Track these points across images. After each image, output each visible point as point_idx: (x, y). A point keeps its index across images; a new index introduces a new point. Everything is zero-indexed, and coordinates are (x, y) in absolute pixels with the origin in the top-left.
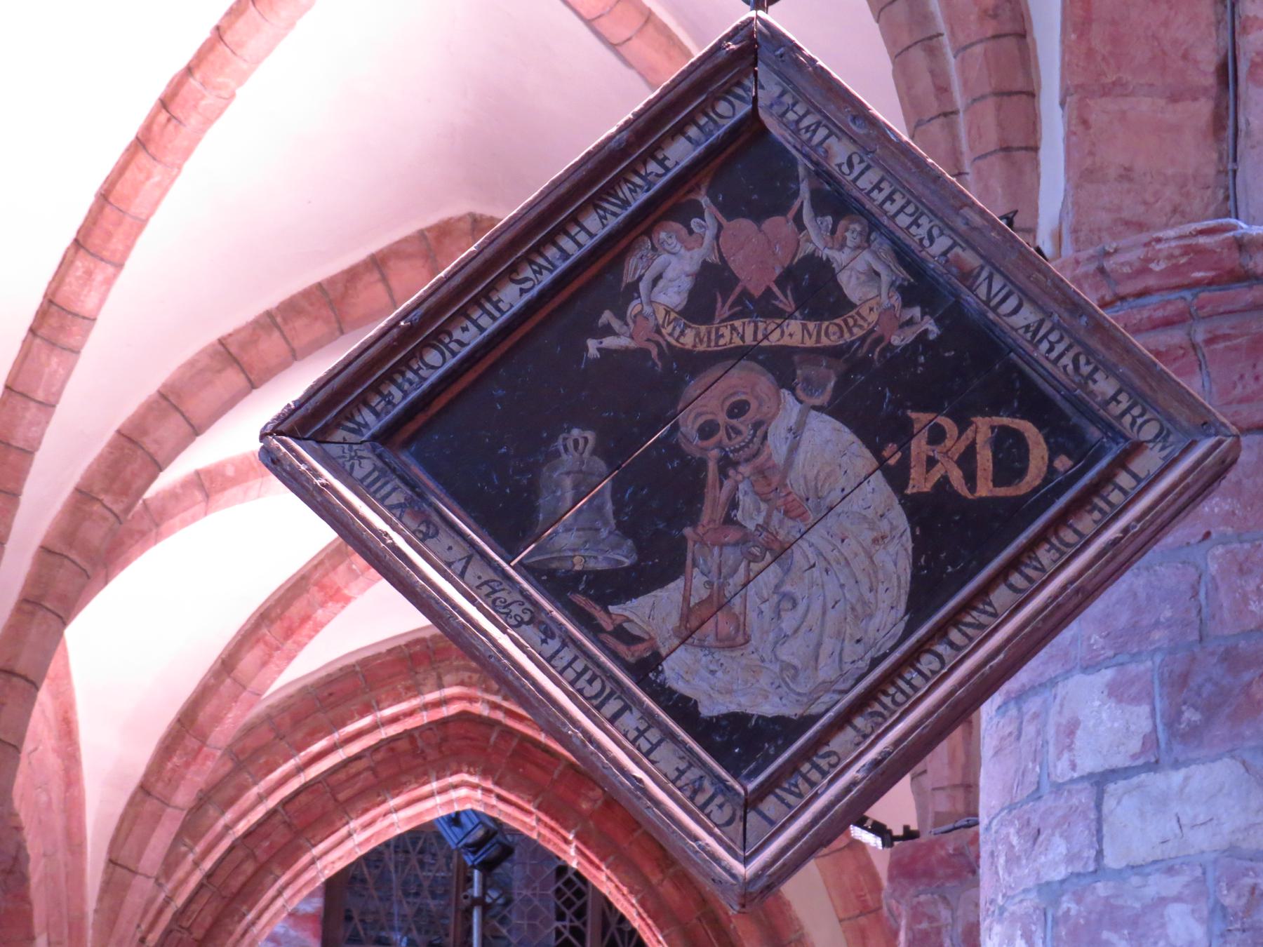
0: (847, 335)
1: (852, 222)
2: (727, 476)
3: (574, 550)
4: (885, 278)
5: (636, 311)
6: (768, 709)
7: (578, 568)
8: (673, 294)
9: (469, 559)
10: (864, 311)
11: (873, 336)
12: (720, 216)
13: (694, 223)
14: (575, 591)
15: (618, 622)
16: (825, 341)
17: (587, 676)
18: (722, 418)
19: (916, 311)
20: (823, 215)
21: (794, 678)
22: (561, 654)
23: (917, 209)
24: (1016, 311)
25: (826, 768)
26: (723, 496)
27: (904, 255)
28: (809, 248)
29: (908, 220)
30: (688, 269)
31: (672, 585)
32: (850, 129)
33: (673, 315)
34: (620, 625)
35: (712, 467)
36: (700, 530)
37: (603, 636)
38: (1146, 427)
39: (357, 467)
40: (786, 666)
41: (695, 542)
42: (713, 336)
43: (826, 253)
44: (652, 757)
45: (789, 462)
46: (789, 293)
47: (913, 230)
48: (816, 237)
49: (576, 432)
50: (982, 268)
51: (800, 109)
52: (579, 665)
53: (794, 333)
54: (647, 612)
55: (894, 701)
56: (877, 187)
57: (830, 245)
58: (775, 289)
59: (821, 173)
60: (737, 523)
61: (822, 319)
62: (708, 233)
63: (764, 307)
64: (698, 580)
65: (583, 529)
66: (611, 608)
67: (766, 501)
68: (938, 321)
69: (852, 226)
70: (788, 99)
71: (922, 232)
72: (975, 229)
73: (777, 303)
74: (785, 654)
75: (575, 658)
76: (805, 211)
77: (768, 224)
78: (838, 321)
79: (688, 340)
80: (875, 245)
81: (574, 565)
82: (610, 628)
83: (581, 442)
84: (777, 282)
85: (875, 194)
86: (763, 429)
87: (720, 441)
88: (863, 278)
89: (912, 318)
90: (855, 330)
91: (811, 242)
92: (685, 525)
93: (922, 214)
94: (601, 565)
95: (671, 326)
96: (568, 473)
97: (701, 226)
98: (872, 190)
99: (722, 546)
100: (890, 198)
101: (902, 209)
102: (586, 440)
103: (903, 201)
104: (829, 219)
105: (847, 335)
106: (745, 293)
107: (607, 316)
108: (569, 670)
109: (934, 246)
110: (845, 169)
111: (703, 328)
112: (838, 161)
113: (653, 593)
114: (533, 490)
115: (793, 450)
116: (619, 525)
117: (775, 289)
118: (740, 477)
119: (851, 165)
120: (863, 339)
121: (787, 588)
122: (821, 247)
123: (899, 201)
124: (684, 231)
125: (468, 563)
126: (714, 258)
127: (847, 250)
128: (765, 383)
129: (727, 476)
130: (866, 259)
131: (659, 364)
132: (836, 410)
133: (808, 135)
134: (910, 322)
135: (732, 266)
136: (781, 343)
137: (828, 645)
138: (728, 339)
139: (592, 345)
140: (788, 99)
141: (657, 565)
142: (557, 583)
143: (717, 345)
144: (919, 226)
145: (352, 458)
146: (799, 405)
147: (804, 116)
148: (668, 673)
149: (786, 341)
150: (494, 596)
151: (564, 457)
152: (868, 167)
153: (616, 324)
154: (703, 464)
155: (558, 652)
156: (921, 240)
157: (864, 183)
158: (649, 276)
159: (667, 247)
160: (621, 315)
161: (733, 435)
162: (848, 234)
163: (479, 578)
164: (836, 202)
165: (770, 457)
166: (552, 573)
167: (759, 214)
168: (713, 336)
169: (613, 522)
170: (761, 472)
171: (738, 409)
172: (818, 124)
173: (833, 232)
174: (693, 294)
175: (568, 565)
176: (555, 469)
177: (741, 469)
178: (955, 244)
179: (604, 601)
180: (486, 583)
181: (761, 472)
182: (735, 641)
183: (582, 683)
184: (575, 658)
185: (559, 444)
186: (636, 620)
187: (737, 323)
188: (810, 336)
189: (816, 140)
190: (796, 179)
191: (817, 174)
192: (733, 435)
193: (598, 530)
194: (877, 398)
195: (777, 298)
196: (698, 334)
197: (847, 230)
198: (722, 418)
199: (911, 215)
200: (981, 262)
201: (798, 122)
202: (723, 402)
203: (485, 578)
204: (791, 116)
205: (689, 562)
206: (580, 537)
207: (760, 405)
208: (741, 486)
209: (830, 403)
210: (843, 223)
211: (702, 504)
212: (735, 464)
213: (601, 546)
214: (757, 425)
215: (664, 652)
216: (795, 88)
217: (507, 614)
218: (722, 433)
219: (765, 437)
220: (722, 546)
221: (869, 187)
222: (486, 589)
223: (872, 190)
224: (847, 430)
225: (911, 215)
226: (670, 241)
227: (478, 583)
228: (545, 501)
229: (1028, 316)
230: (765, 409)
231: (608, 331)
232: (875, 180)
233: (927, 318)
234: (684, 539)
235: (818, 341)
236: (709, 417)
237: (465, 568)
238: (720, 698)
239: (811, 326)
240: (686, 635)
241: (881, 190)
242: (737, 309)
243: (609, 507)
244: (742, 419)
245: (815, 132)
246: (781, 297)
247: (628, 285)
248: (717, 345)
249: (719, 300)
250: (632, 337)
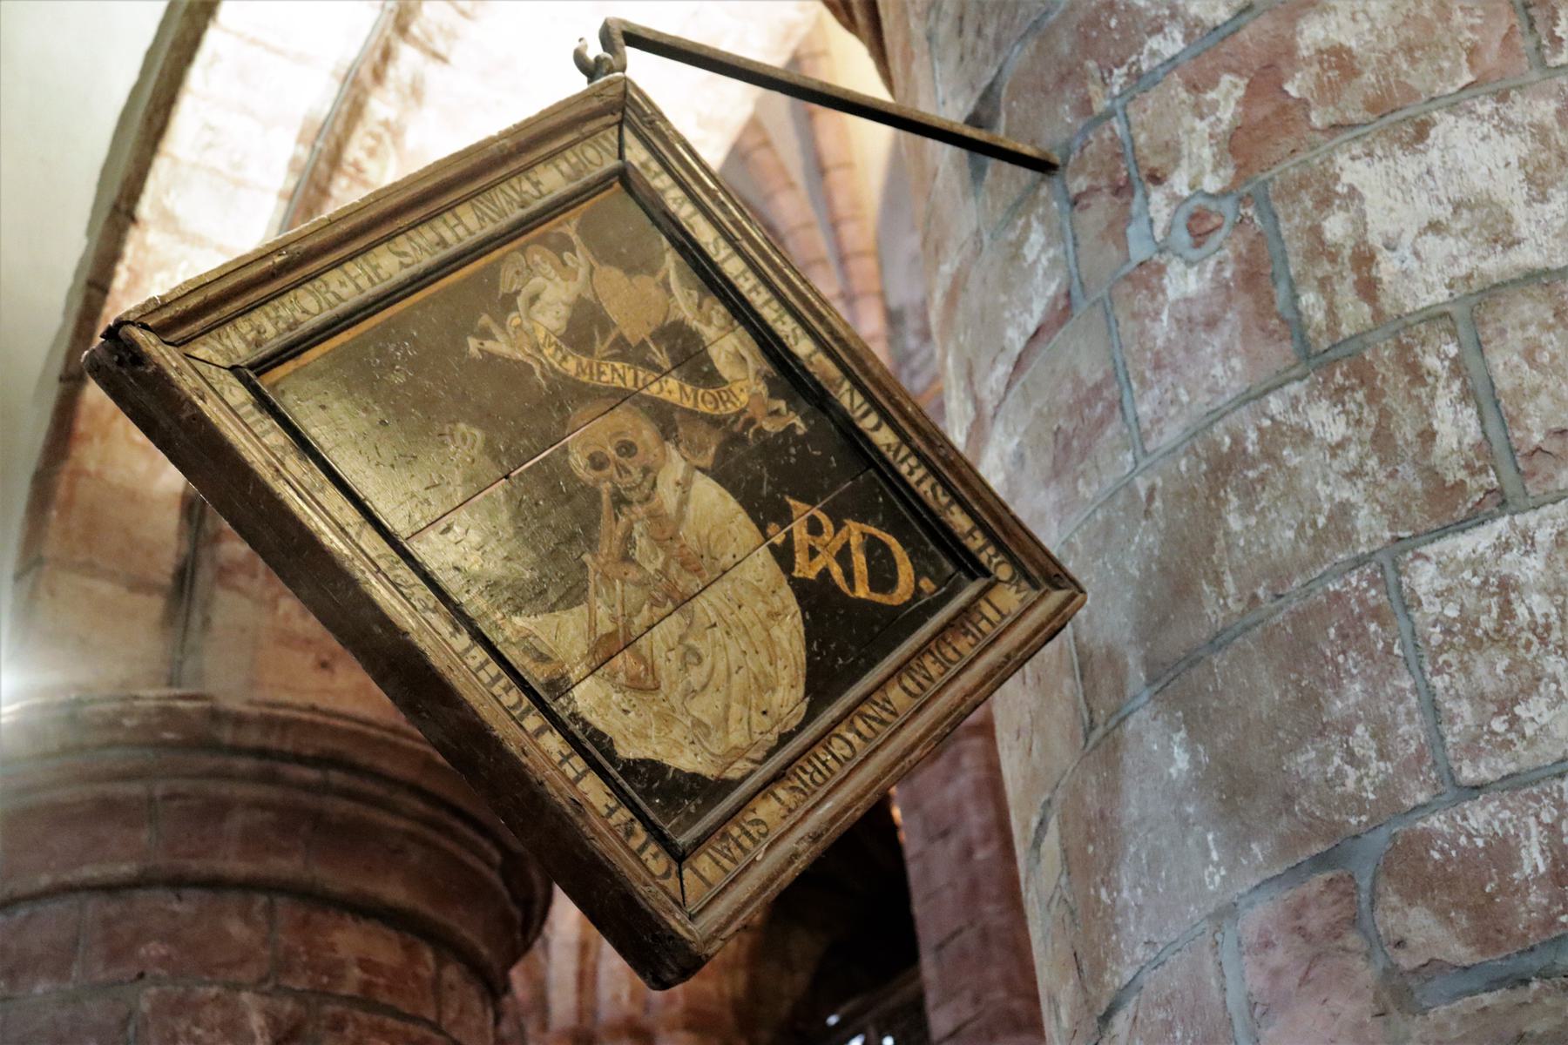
18: (611, 451)
30: (564, 297)
40: (698, 723)
45: (681, 515)
79: (571, 366)
84: (652, 337)
86: (651, 475)
107: (485, 319)
121: (691, 641)
124: (557, 262)
132: (722, 475)
137: (736, 709)
139: (473, 344)
153: (495, 330)
158: (526, 292)
170: (653, 516)
174: (572, 324)
198: (611, 451)
212: (629, 503)
215: (573, 677)
218: (611, 470)
219: (654, 485)
231: (486, 334)
238: (636, 742)
242: (615, 351)
247: (505, 296)
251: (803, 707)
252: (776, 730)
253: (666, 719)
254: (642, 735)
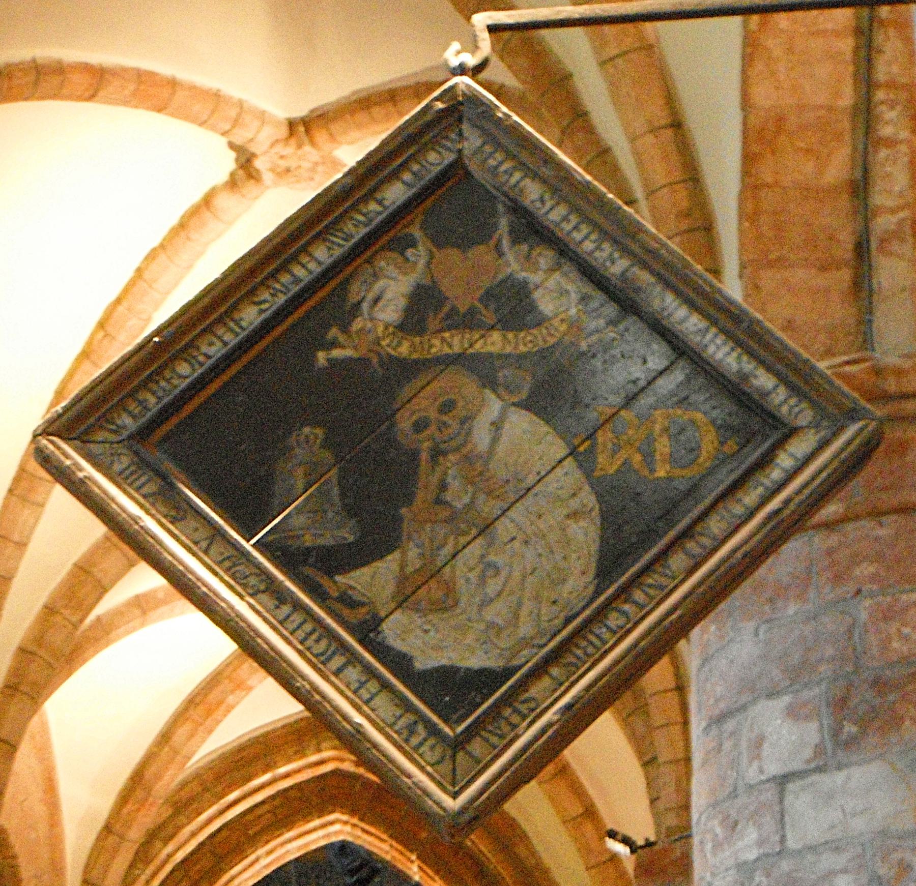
6: (475, 662)
7: (308, 544)
8: (390, 313)
18: (433, 414)
21: (498, 635)
25: (526, 712)
26: (435, 479)
33: (391, 329)
35: (424, 456)
36: (414, 508)
38: (800, 416)
40: (491, 625)
44: (372, 703)
48: (513, 263)
49: (307, 430)
55: (586, 653)
56: (565, 219)
64: (413, 553)
67: (472, 483)
74: (489, 614)
79: (404, 350)
82: (336, 594)
84: (481, 300)
94: (327, 540)
101: (586, 237)
107: (334, 332)
110: (538, 204)
114: (269, 478)
115: (495, 440)
116: (345, 506)
121: (492, 558)
124: (400, 259)
126: (426, 282)
133: (507, 177)
137: (528, 606)
138: (437, 347)
139: (321, 357)
143: (429, 353)
148: (387, 632)
149: (490, 349)
150: (233, 570)
153: (342, 338)
155: (288, 616)
158: (370, 296)
160: (345, 329)
163: (222, 554)
167: (464, 243)
170: (468, 459)
177: (451, 457)
179: (330, 573)
180: (228, 558)
182: (446, 603)
183: (309, 643)
185: (292, 440)
186: (359, 587)
187: (447, 335)
189: (513, 180)
198: (433, 414)
203: (226, 554)
205: (404, 538)
212: (444, 453)
215: (383, 614)
218: (433, 428)
222: (227, 564)
227: (221, 558)
228: (278, 489)
231: (334, 344)
235: (516, 348)
236: (423, 414)
238: (434, 654)
239: (510, 335)
240: (404, 599)
243: (336, 491)
245: (511, 175)
250: (355, 348)
251: (592, 588)
252: (562, 615)
253: (462, 629)
254: (438, 648)
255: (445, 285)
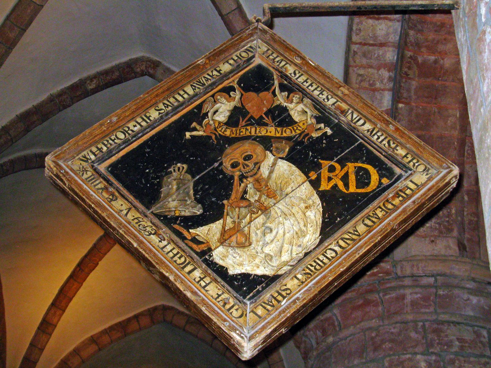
0: (294, 133)
1: (296, 94)
2: (242, 182)
3: (176, 208)
4: (309, 113)
5: (206, 123)
6: (260, 271)
7: (177, 215)
8: (222, 117)
9: (130, 209)
10: (301, 124)
11: (305, 133)
12: (242, 91)
13: (232, 93)
14: (175, 223)
15: (193, 236)
16: (284, 135)
17: (178, 256)
18: (241, 161)
19: (322, 125)
20: (284, 91)
21: (271, 260)
22: (168, 247)
23: (322, 89)
24: (363, 124)
25: (285, 295)
26: (241, 189)
27: (317, 105)
28: (278, 103)
29: (318, 93)
30: (228, 109)
31: (218, 222)
32: (295, 61)
33: (222, 124)
34: (194, 238)
35: (236, 178)
36: (231, 201)
37: (186, 241)
38: (419, 167)
39: (85, 174)
40: (267, 255)
41: (228, 206)
42: (238, 132)
43: (285, 104)
44: (206, 288)
45: (269, 177)
46: (270, 117)
47: (321, 96)
48: (281, 99)
49: (179, 165)
50: (349, 109)
51: (275, 55)
52: (175, 251)
53: (271, 131)
54: (206, 232)
55: (315, 269)
56: (306, 81)
57: (287, 102)
58: (264, 116)
59: (283, 76)
60: (246, 199)
61: (284, 127)
62: (237, 97)
63: (260, 123)
64: (229, 220)
65: (180, 200)
66: (190, 230)
67: (259, 191)
68: (331, 129)
69: (295, 96)
70: (270, 52)
71: (324, 97)
72: (345, 95)
73: (264, 121)
74: (267, 250)
75: (174, 249)
76: (276, 91)
77: (262, 94)
78: (289, 128)
79: (228, 133)
80: (305, 102)
81: (175, 214)
82: (190, 238)
83: (181, 168)
84: (265, 114)
85: (305, 83)
86: (258, 165)
87: (240, 169)
88: (300, 113)
89: (320, 127)
90: (297, 131)
91: (279, 100)
92: (224, 200)
93: (324, 91)
94: (187, 214)
95: (221, 128)
96: (175, 180)
97: (234, 94)
98: (304, 82)
99: (239, 208)
100: (311, 85)
101: (316, 89)
102: (183, 168)
103: (316, 87)
104: (286, 93)
105: (294, 133)
106: (252, 117)
107: (194, 124)
108: (171, 253)
109: (329, 101)
110: (293, 75)
111: (234, 129)
112: (290, 72)
113: (209, 225)
114: (160, 185)
115: (271, 172)
116: (196, 199)
117: (264, 116)
118: (248, 182)
119: (295, 74)
120: (300, 134)
121: (268, 225)
122: (283, 102)
123: (315, 86)
124: (227, 96)
125: (129, 211)
126: (239, 105)
127: (293, 104)
128: (259, 149)
129: (242, 182)
130: (300, 107)
131: (215, 141)
132: (290, 158)
133: (278, 63)
134: (320, 129)
135: (246, 108)
136: (266, 135)
137: (286, 247)
138: (244, 133)
139: (188, 135)
140: (270, 52)
141: (212, 213)
142: (168, 221)
143: (240, 135)
144: (323, 95)
145: (83, 171)
146: (274, 157)
147: (276, 57)
148: (214, 256)
149: (268, 134)
150: (139, 224)
151: (174, 174)
152: (302, 75)
153: (198, 127)
154: (232, 177)
155: (166, 246)
156: (324, 100)
157: (301, 80)
158: (212, 111)
159: (220, 101)
160: (200, 124)
161: (246, 167)
162: (294, 98)
163: (134, 216)
164: (289, 87)
165: (261, 175)
166: (165, 217)
167: (257, 91)
168: (238, 132)
169: (193, 198)
170: (258, 181)
171: (248, 158)
172: (282, 60)
173: (288, 97)
174: (230, 117)
175: (173, 213)
176: (170, 177)
177: (249, 179)
178: (337, 101)
179: (188, 228)
180: (136, 218)
181: (258, 181)
182: (245, 244)
183: (176, 258)
184: (174, 249)
185: (171, 169)
186: (200, 234)
187: (249, 128)
188: (278, 133)
189: (281, 65)
190: (273, 80)
191: (282, 77)
192: (246, 167)
193: (186, 201)
194: (305, 155)
195: (264, 119)
196: (232, 131)
197: (294, 97)
198: (241, 161)
199: (320, 91)
200: (349, 107)
201: (274, 59)
202: (242, 155)
203: (135, 217)
204: (271, 57)
205: (225, 213)
206: (179, 203)
207: (257, 156)
208: (248, 186)
209: (286, 157)
210: (291, 95)
211: (232, 192)
212: (246, 178)
213: (187, 207)
214: (256, 164)
215: (213, 248)
216: (273, 48)
217: (145, 230)
218: (241, 167)
219: (259, 168)
220: (239, 208)
221: (302, 81)
222: (136, 221)
223: (304, 82)
224: (294, 166)
225: (320, 91)
226: (221, 99)
227: (133, 218)
228: (164, 190)
229: (368, 126)
230: (259, 158)
231: (195, 129)
232: (305, 79)
233: (327, 128)
234: (223, 205)
235: (282, 134)
236: (236, 160)
237: (127, 213)
238: (238, 267)
239: (279, 129)
240: (224, 240)
241: (307, 82)
242: (248, 123)
243: (192, 192)
244: (249, 161)
245: (281, 63)
246: (266, 119)
247: (204, 114)
248: (240, 135)
249: (241, 119)
250: (204, 131)
251: (318, 240)
252: (304, 252)
253: (254, 257)
254: (241, 264)
255: (248, 106)
